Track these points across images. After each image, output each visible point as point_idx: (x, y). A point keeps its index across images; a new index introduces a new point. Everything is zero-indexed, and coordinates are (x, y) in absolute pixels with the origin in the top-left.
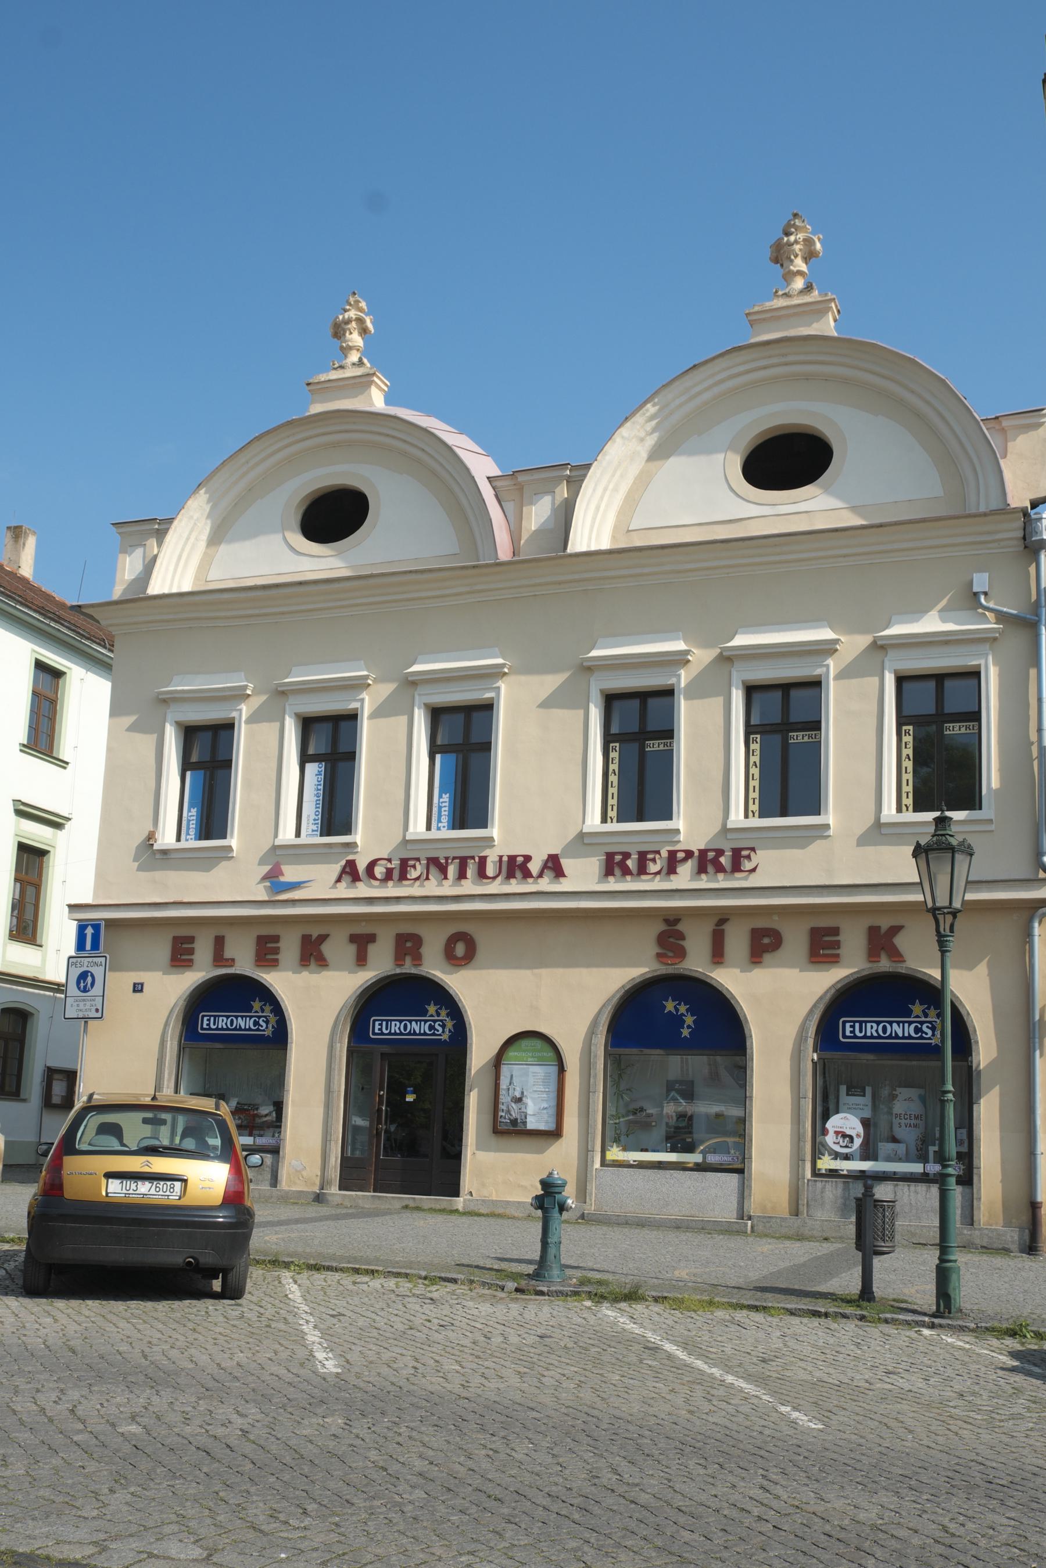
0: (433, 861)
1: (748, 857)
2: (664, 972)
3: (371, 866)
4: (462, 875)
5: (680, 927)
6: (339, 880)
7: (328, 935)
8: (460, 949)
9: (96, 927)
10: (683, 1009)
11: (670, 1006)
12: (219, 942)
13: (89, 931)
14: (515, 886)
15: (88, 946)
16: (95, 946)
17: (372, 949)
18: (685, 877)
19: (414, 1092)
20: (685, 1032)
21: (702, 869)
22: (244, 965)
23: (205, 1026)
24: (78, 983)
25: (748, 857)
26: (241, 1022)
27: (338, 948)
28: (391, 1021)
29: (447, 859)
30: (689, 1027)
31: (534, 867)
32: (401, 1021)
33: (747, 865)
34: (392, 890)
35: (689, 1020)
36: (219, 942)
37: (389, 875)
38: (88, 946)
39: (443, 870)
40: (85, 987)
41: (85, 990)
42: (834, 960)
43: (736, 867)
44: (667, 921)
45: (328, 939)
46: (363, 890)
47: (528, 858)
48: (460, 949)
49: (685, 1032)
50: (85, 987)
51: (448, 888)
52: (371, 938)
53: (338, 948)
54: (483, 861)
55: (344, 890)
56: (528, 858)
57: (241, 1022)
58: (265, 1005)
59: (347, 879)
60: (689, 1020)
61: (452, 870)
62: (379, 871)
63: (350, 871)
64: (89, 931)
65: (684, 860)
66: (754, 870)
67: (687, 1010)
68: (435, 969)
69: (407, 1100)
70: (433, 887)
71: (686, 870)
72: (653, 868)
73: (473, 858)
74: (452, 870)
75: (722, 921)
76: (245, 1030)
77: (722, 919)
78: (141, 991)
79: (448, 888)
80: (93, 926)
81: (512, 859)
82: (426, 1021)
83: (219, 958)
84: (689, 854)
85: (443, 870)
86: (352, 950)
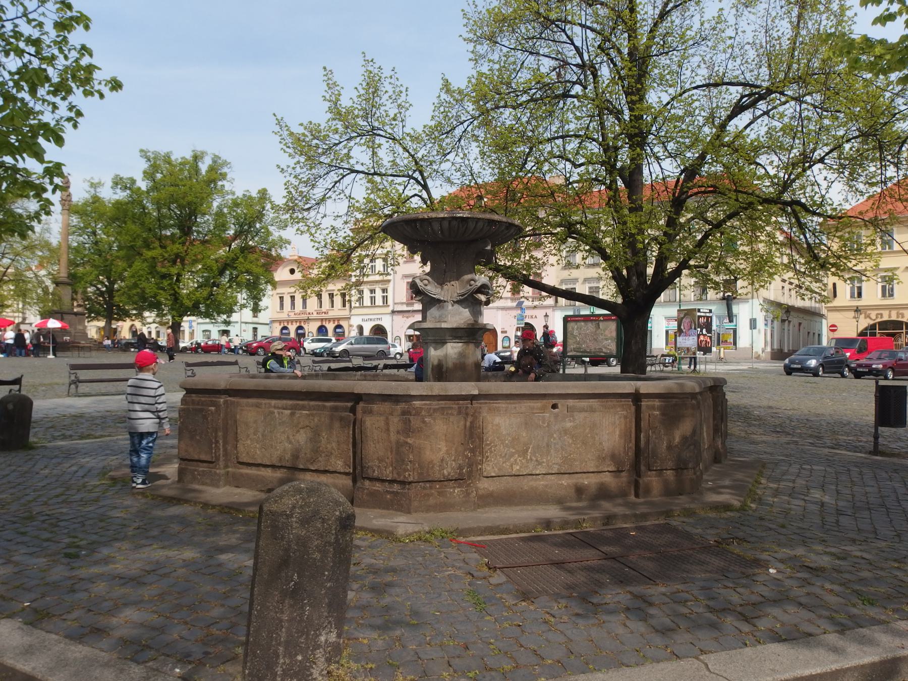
22: (286, 324)
68: (302, 325)
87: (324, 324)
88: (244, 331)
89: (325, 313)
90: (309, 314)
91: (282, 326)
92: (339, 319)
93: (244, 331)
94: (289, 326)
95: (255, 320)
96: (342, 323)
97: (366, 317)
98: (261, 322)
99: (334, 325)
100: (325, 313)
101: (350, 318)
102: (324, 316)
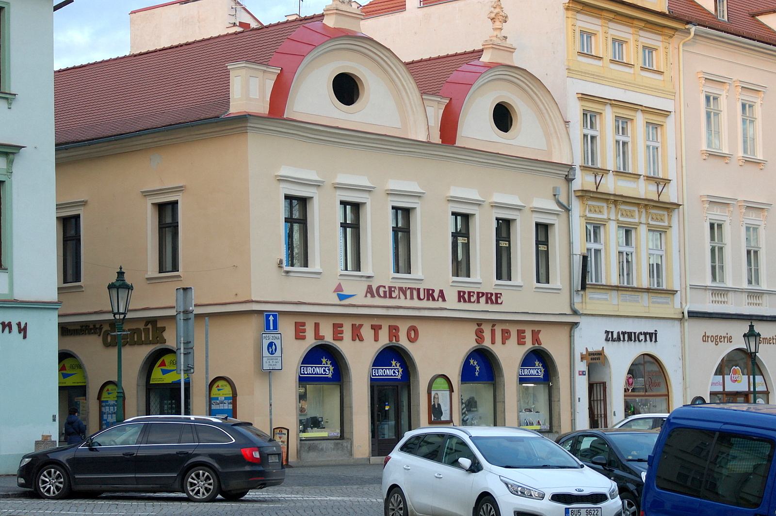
0: (401, 289)
4: (412, 298)
5: (482, 327)
6: (366, 296)
7: (363, 325)
9: (274, 316)
10: (475, 363)
12: (317, 326)
13: (271, 318)
14: (431, 304)
15: (272, 328)
16: (275, 328)
17: (381, 332)
19: (388, 405)
20: (477, 373)
21: (487, 302)
24: (268, 349)
25: (500, 297)
26: (318, 370)
27: (367, 332)
28: (379, 369)
29: (406, 288)
30: (478, 371)
35: (478, 368)
36: (317, 326)
37: (385, 297)
38: (272, 328)
40: (272, 351)
42: (524, 344)
43: (497, 303)
45: (363, 327)
47: (433, 291)
49: (477, 373)
50: (272, 351)
51: (408, 303)
52: (380, 327)
53: (367, 332)
54: (418, 290)
55: (369, 301)
57: (318, 370)
58: (327, 360)
59: (369, 295)
60: (478, 368)
61: (408, 292)
64: (271, 318)
65: (482, 296)
66: (501, 303)
68: (404, 342)
69: (386, 409)
70: (402, 302)
72: (472, 299)
73: (415, 289)
75: (494, 326)
77: (494, 323)
79: (408, 303)
80: (272, 315)
81: (428, 290)
82: (392, 369)
83: (317, 336)
90: (430, 294)
97: (618, 327)
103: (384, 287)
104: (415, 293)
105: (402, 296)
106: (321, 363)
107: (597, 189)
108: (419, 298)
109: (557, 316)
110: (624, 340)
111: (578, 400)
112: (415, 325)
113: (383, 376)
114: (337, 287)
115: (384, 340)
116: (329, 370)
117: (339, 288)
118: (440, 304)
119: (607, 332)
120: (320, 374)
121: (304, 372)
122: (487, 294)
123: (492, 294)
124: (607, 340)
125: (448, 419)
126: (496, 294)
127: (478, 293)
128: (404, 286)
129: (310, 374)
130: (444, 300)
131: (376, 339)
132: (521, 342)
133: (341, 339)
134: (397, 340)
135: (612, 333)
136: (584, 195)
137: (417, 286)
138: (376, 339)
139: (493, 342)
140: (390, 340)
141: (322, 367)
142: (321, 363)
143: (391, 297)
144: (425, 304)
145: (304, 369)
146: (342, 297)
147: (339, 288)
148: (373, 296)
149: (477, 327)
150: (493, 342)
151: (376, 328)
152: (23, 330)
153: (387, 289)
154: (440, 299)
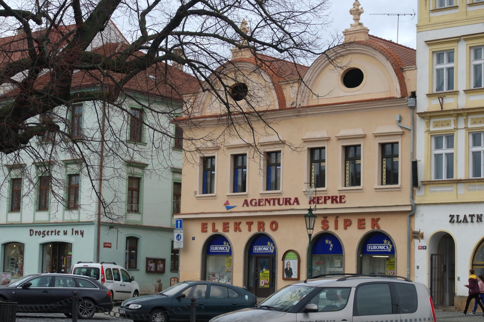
0: (266, 200)
1: (343, 198)
2: (324, 232)
3: (251, 201)
4: (274, 204)
5: (327, 219)
6: (243, 206)
8: (274, 226)
9: (181, 221)
10: (330, 242)
11: (327, 241)
12: (214, 225)
13: (179, 222)
14: (288, 207)
15: (179, 227)
16: (181, 227)
17: (252, 226)
18: (329, 204)
20: (331, 249)
21: (332, 202)
22: (220, 230)
23: (369, 249)
24: (177, 238)
25: (343, 198)
26: (221, 248)
27: (244, 226)
29: (270, 199)
30: (331, 248)
31: (292, 202)
32: (261, 247)
33: (343, 201)
34: (258, 208)
35: (332, 246)
36: (214, 225)
37: (256, 205)
38: (179, 227)
39: (269, 203)
41: (179, 240)
42: (364, 228)
43: (341, 202)
44: (324, 217)
46: (251, 208)
47: (290, 199)
48: (274, 226)
49: (331, 249)
52: (252, 223)
53: (244, 226)
54: (279, 200)
55: (246, 208)
56: (290, 199)
57: (221, 248)
59: (245, 205)
60: (332, 246)
61: (272, 202)
62: (253, 203)
63: (246, 202)
64: (179, 222)
66: (344, 202)
67: (331, 243)
68: (268, 231)
70: (267, 207)
71: (329, 202)
72: (320, 202)
73: (276, 199)
74: (272, 202)
75: (337, 217)
76: (382, 250)
77: (337, 216)
78: (194, 239)
79: (272, 207)
80: (180, 221)
81: (286, 199)
82: (267, 247)
83: (214, 230)
84: (329, 197)
85: (269, 203)
86: (247, 226)
87: (331, 229)
88: (107, 245)
89: (334, 199)
90: (287, 201)
91: (210, 233)
92: (376, 217)
93: (107, 245)
94: (231, 235)
95: (134, 218)
96: (385, 226)
97: (462, 212)
98: (146, 223)
99: (361, 234)
100: (334, 199)
101: (411, 214)
102: (330, 207)
103: (256, 200)
104: (276, 201)
105: (267, 204)
106: (383, 243)
107: (442, 108)
108: (279, 204)
109: (357, 209)
110: (472, 221)
111: (416, 267)
112: (274, 220)
113: (261, 251)
114: (226, 202)
115: (255, 230)
116: (389, 247)
117: (227, 203)
118: (295, 206)
119: (452, 216)
120: (382, 250)
121: (370, 248)
122: (333, 197)
123: (337, 197)
124: (451, 221)
125: (296, 277)
126: (341, 197)
127: (325, 197)
128: (268, 198)
129: (375, 250)
130: (298, 203)
131: (250, 230)
132: (361, 225)
133: (228, 231)
134: (264, 230)
135: (458, 216)
136: (427, 116)
137: (277, 197)
138: (250, 230)
139: (336, 228)
140: (259, 230)
141: (384, 245)
142: (383, 243)
143: (259, 205)
144: (284, 207)
145: (370, 247)
146: (228, 208)
147: (227, 203)
148: (248, 205)
149: (323, 219)
150: (336, 228)
151: (250, 224)
152: (82, 234)
153: (257, 201)
154: (295, 204)
